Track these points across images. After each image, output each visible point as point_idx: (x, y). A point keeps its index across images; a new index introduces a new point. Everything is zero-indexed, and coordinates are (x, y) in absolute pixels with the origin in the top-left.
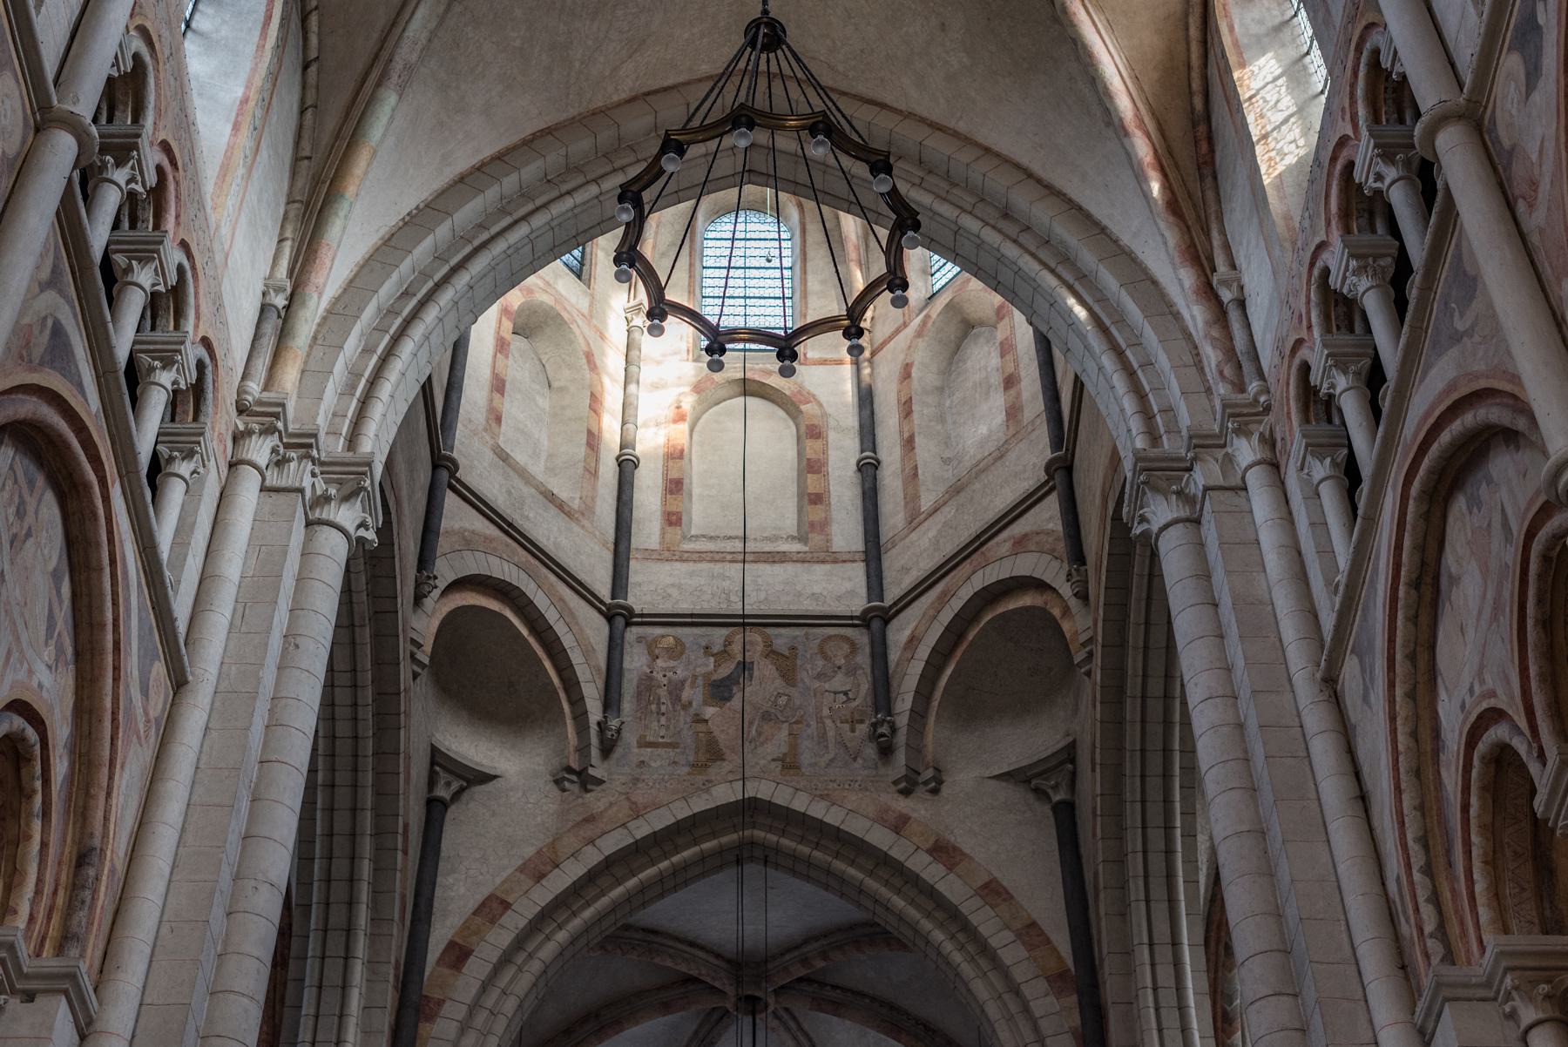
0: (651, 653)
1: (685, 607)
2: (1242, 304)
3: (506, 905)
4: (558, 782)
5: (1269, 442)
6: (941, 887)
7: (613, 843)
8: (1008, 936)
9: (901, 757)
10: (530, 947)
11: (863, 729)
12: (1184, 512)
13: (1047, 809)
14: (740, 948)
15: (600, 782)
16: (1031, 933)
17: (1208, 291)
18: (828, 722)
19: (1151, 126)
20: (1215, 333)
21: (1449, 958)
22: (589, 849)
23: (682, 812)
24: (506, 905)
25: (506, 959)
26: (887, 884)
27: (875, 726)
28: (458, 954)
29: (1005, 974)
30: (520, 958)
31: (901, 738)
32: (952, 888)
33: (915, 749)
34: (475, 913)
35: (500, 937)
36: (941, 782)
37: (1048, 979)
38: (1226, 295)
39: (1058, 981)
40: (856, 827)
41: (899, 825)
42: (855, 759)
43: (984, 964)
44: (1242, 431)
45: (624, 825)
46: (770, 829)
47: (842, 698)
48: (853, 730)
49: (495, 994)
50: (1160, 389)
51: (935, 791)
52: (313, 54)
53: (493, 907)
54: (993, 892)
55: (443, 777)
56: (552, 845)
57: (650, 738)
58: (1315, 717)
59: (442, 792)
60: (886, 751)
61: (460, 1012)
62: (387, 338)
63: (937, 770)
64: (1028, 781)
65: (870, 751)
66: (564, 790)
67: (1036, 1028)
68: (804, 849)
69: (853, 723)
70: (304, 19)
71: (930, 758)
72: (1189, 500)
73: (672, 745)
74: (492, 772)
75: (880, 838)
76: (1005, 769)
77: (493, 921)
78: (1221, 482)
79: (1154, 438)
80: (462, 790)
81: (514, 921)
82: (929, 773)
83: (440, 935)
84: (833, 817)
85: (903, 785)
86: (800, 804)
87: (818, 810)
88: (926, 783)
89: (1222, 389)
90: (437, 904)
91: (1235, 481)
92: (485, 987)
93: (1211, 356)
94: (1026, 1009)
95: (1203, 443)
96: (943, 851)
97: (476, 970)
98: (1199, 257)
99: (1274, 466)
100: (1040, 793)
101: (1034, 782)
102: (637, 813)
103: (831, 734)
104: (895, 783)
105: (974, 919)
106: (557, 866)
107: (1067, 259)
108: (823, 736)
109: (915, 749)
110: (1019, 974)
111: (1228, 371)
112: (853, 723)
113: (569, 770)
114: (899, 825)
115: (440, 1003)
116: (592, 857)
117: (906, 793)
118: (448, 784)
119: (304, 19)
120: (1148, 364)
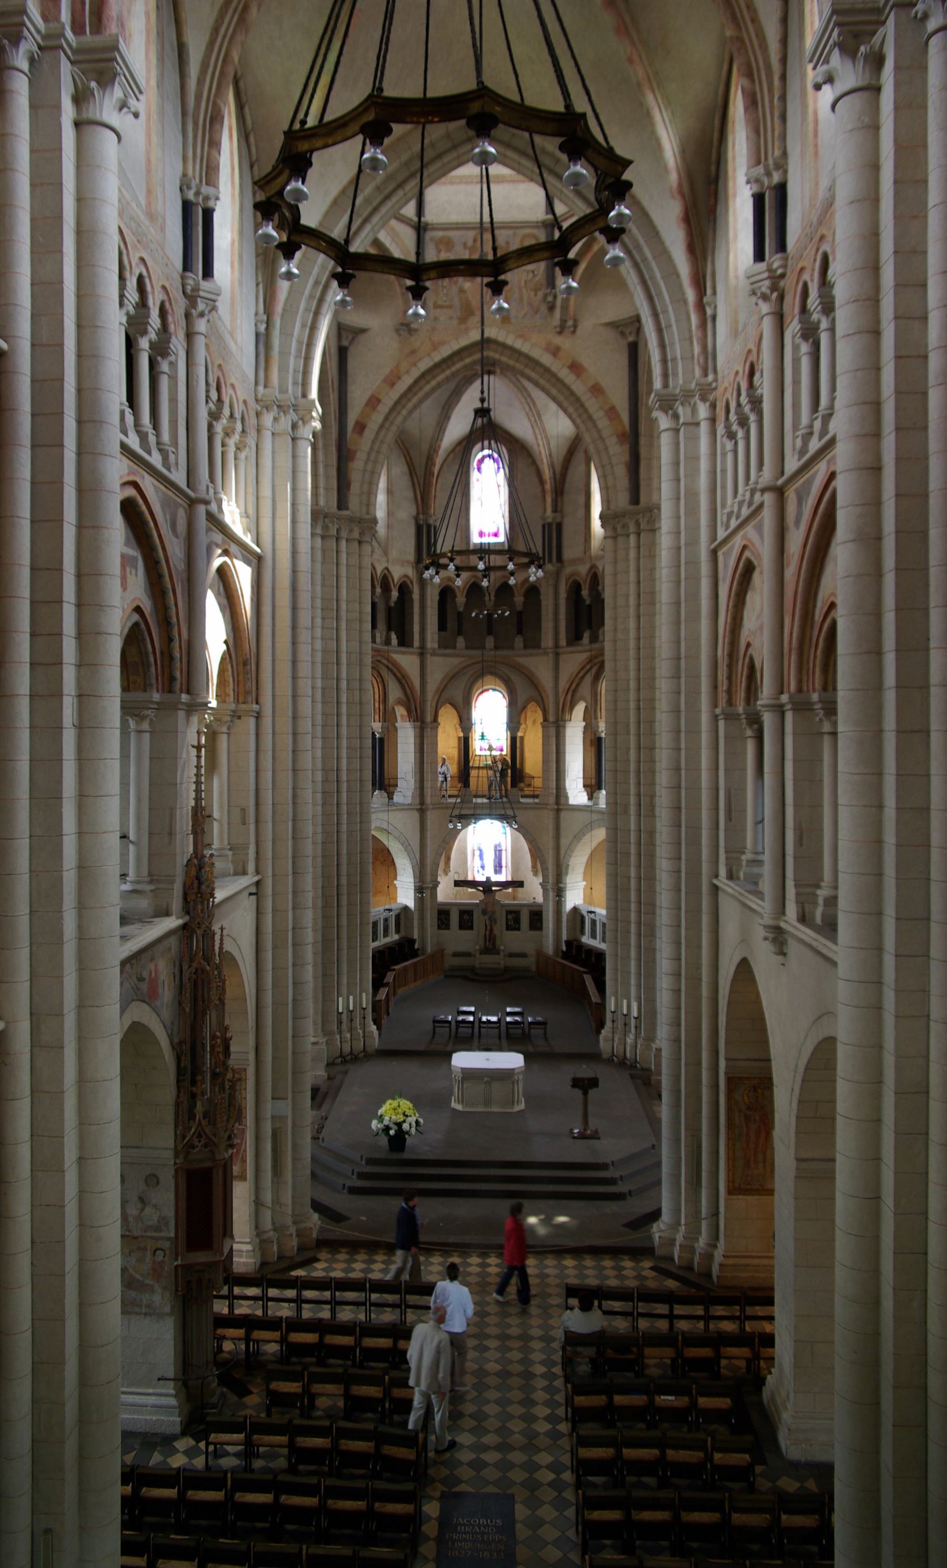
0: (437, 247)
1: (454, 218)
2: (714, 318)
3: (379, 401)
4: (397, 331)
5: (713, 406)
6: (574, 387)
7: (425, 365)
8: (601, 414)
9: (557, 313)
10: (391, 418)
11: (540, 294)
12: (673, 426)
13: (623, 344)
14: (486, 218)
15: (416, 330)
16: (611, 412)
17: (701, 306)
18: (524, 291)
19: (686, 189)
20: (700, 334)
21: (730, 702)
22: (414, 369)
23: (455, 346)
24: (379, 401)
25: (382, 426)
26: (548, 381)
27: (546, 296)
28: (361, 427)
29: (599, 431)
30: (387, 425)
31: (559, 303)
32: (578, 387)
33: (565, 308)
34: (367, 405)
35: (376, 419)
36: (575, 326)
37: (618, 436)
38: (709, 312)
39: (622, 437)
40: (537, 354)
41: (555, 351)
42: (536, 313)
43: (590, 424)
44: (703, 399)
45: (429, 355)
46: (496, 351)
47: (531, 275)
48: (536, 295)
49: (378, 444)
50: (672, 344)
51: (574, 332)
52: (254, 158)
53: (373, 402)
54: (597, 390)
55: (344, 334)
56: (397, 367)
57: (440, 303)
58: (705, 568)
59: (345, 343)
60: (552, 308)
61: (364, 456)
62: (312, 314)
63: (575, 321)
64: (618, 327)
65: (544, 309)
66: (400, 335)
67: (609, 458)
68: (511, 363)
69: (536, 291)
70: (247, 138)
71: (571, 313)
72: (676, 417)
73: (450, 307)
74: (365, 327)
75: (546, 359)
76: (607, 321)
77: (374, 408)
78: (689, 420)
79: (666, 385)
80: (353, 339)
81: (383, 409)
82: (570, 323)
83: (352, 417)
84: (525, 348)
85: (558, 330)
86: (509, 341)
87: (518, 345)
88: (570, 327)
89: (698, 372)
90: (349, 401)
91: (695, 421)
92: (373, 442)
93: (697, 349)
94: (606, 448)
95: (687, 396)
96: (576, 368)
97: (369, 434)
98: (699, 282)
99: (713, 420)
100: (623, 334)
101: (620, 328)
102: (435, 347)
103: (525, 298)
104: (555, 327)
105: (587, 405)
106: (399, 378)
107: (638, 247)
108: (521, 299)
109: (565, 308)
110: (605, 433)
111: (701, 360)
112: (536, 291)
113: (402, 324)
114: (555, 351)
115: (355, 452)
116: (415, 373)
117: (560, 333)
118: (347, 337)
119: (247, 138)
120: (669, 326)
